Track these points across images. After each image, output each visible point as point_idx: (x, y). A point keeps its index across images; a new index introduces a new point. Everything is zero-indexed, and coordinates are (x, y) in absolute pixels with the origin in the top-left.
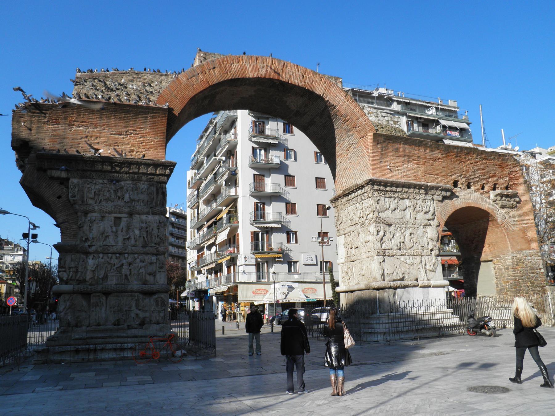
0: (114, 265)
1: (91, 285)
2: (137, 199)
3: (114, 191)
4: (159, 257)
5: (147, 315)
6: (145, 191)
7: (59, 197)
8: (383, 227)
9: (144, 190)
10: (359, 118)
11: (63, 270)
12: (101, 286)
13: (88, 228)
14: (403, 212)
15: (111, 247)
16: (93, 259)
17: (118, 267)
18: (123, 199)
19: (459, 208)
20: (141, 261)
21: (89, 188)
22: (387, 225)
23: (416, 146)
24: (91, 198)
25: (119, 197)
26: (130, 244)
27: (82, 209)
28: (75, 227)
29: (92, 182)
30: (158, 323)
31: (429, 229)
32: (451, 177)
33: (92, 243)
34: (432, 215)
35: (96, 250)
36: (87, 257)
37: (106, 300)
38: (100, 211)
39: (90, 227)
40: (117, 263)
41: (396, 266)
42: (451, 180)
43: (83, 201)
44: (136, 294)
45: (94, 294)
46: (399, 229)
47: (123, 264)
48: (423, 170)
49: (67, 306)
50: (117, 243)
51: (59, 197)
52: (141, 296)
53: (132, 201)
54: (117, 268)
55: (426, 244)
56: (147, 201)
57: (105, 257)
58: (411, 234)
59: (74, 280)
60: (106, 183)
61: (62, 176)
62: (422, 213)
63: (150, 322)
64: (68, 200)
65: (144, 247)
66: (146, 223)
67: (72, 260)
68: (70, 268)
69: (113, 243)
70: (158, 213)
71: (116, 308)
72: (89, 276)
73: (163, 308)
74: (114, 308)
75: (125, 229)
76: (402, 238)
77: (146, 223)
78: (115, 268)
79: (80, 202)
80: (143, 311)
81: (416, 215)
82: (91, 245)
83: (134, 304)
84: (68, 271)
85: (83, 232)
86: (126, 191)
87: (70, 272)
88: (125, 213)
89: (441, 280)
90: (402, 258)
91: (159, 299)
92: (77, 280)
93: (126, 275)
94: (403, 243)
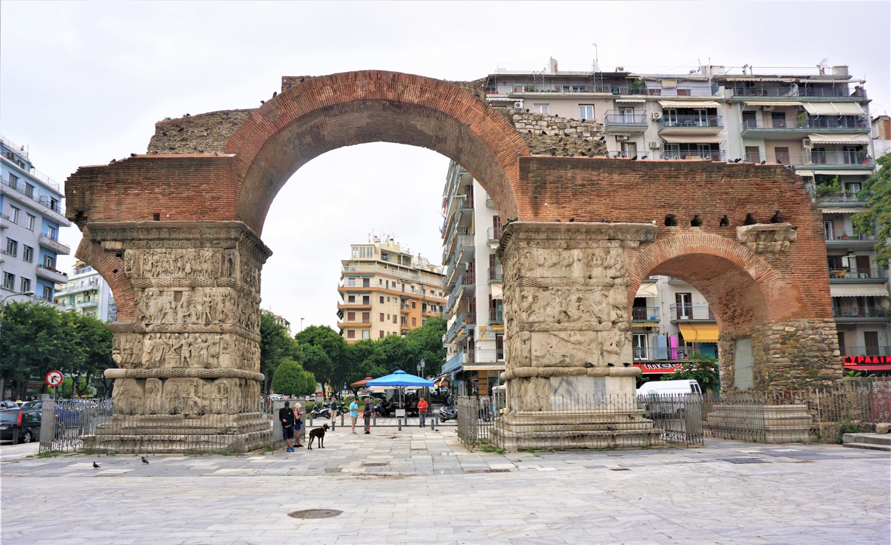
2: (200, 268)
4: (223, 336)
5: (207, 403)
7: (115, 271)
8: (529, 292)
9: (208, 258)
11: (117, 352)
12: (156, 370)
13: (145, 304)
14: (568, 268)
19: (672, 256)
20: (203, 341)
22: (540, 287)
23: (594, 169)
25: (179, 268)
28: (132, 303)
30: (219, 414)
31: (611, 293)
32: (659, 211)
34: (619, 271)
36: (143, 338)
37: (163, 385)
38: (160, 286)
39: (147, 303)
43: (139, 275)
44: (195, 379)
46: (560, 293)
48: (608, 205)
50: (175, 320)
51: (115, 271)
52: (201, 382)
55: (605, 313)
57: (163, 337)
62: (600, 269)
63: (211, 412)
65: (207, 324)
67: (127, 341)
69: (172, 321)
72: (145, 359)
73: (226, 395)
75: (185, 305)
78: (173, 349)
79: (136, 276)
81: (591, 271)
84: (122, 353)
85: (140, 310)
88: (186, 286)
90: (563, 335)
91: (222, 386)
93: (185, 357)
94: (565, 312)
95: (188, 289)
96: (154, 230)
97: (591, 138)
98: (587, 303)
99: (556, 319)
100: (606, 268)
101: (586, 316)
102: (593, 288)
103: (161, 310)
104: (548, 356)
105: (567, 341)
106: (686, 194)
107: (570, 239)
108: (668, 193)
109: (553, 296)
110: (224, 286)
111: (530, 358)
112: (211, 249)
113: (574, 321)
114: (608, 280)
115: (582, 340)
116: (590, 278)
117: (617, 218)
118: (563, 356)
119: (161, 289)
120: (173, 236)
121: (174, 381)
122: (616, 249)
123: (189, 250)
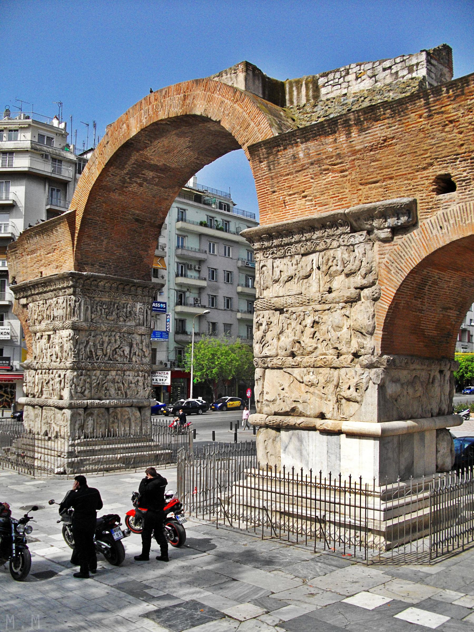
10: (249, 125)
14: (305, 280)
22: (276, 310)
23: (327, 134)
32: (425, 173)
41: (282, 388)
42: (427, 178)
44: (53, 408)
48: (353, 180)
52: (57, 410)
58: (315, 323)
62: (343, 276)
76: (298, 333)
81: (330, 282)
89: (372, 421)
90: (296, 372)
97: (410, 76)
98: (323, 328)
99: (288, 352)
100: (347, 275)
101: (322, 348)
102: (332, 305)
104: (278, 401)
105: (300, 382)
106: (461, 136)
107: (307, 240)
108: (433, 142)
109: (289, 321)
111: (262, 402)
113: (308, 354)
114: (352, 292)
115: (315, 381)
116: (330, 291)
117: (367, 198)
118: (295, 401)
121: (45, 409)
122: (362, 245)
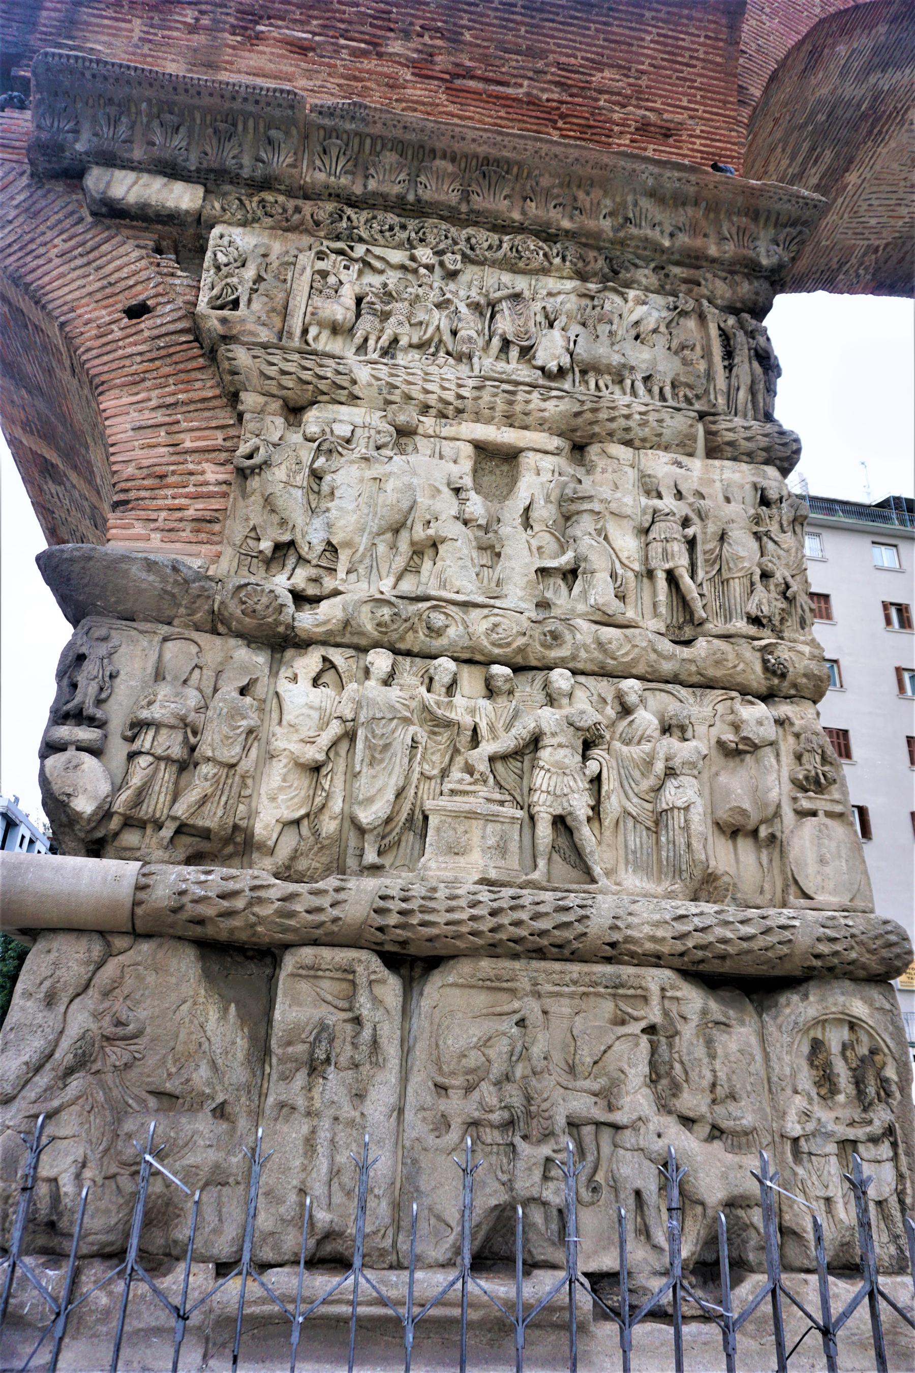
0: (475, 740)
1: (285, 873)
2: (616, 359)
3: (475, 307)
6: (655, 331)
7: (137, 311)
11: (85, 734)
12: (371, 884)
13: (302, 478)
15: (452, 610)
16: (316, 682)
17: (504, 757)
18: (526, 352)
21: (324, 274)
24: (335, 329)
25: (506, 344)
26: (581, 608)
27: (272, 371)
29: (340, 252)
33: (316, 580)
35: (347, 623)
36: (274, 673)
39: (317, 476)
40: (492, 728)
45: (307, 954)
47: (535, 742)
49: (65, 1044)
51: (137, 311)
53: (584, 372)
54: (492, 759)
56: (673, 386)
59: (160, 827)
60: (426, 267)
61: (171, 204)
64: (196, 331)
66: (679, 495)
67: (159, 675)
68: (138, 726)
70: (745, 445)
71: (487, 1092)
74: (469, 1089)
75: (544, 512)
77: (679, 495)
80: (717, 1132)
82: (311, 591)
83: (637, 1072)
84: (118, 749)
86: (540, 318)
87: (132, 756)
88: (541, 425)
91: (835, 1038)
92: (182, 829)
93: (561, 822)
95: (555, 442)
96: (390, 158)
103: (396, 531)
110: (750, 457)
112: (657, 300)
119: (407, 416)
120: (479, 202)
123: (550, 283)
